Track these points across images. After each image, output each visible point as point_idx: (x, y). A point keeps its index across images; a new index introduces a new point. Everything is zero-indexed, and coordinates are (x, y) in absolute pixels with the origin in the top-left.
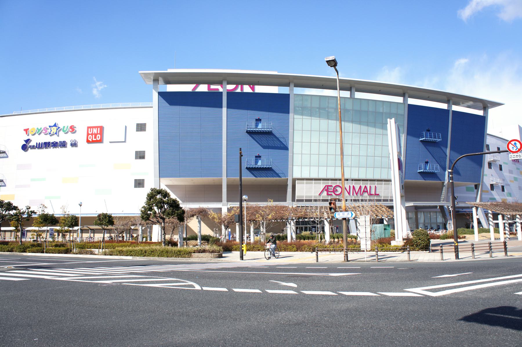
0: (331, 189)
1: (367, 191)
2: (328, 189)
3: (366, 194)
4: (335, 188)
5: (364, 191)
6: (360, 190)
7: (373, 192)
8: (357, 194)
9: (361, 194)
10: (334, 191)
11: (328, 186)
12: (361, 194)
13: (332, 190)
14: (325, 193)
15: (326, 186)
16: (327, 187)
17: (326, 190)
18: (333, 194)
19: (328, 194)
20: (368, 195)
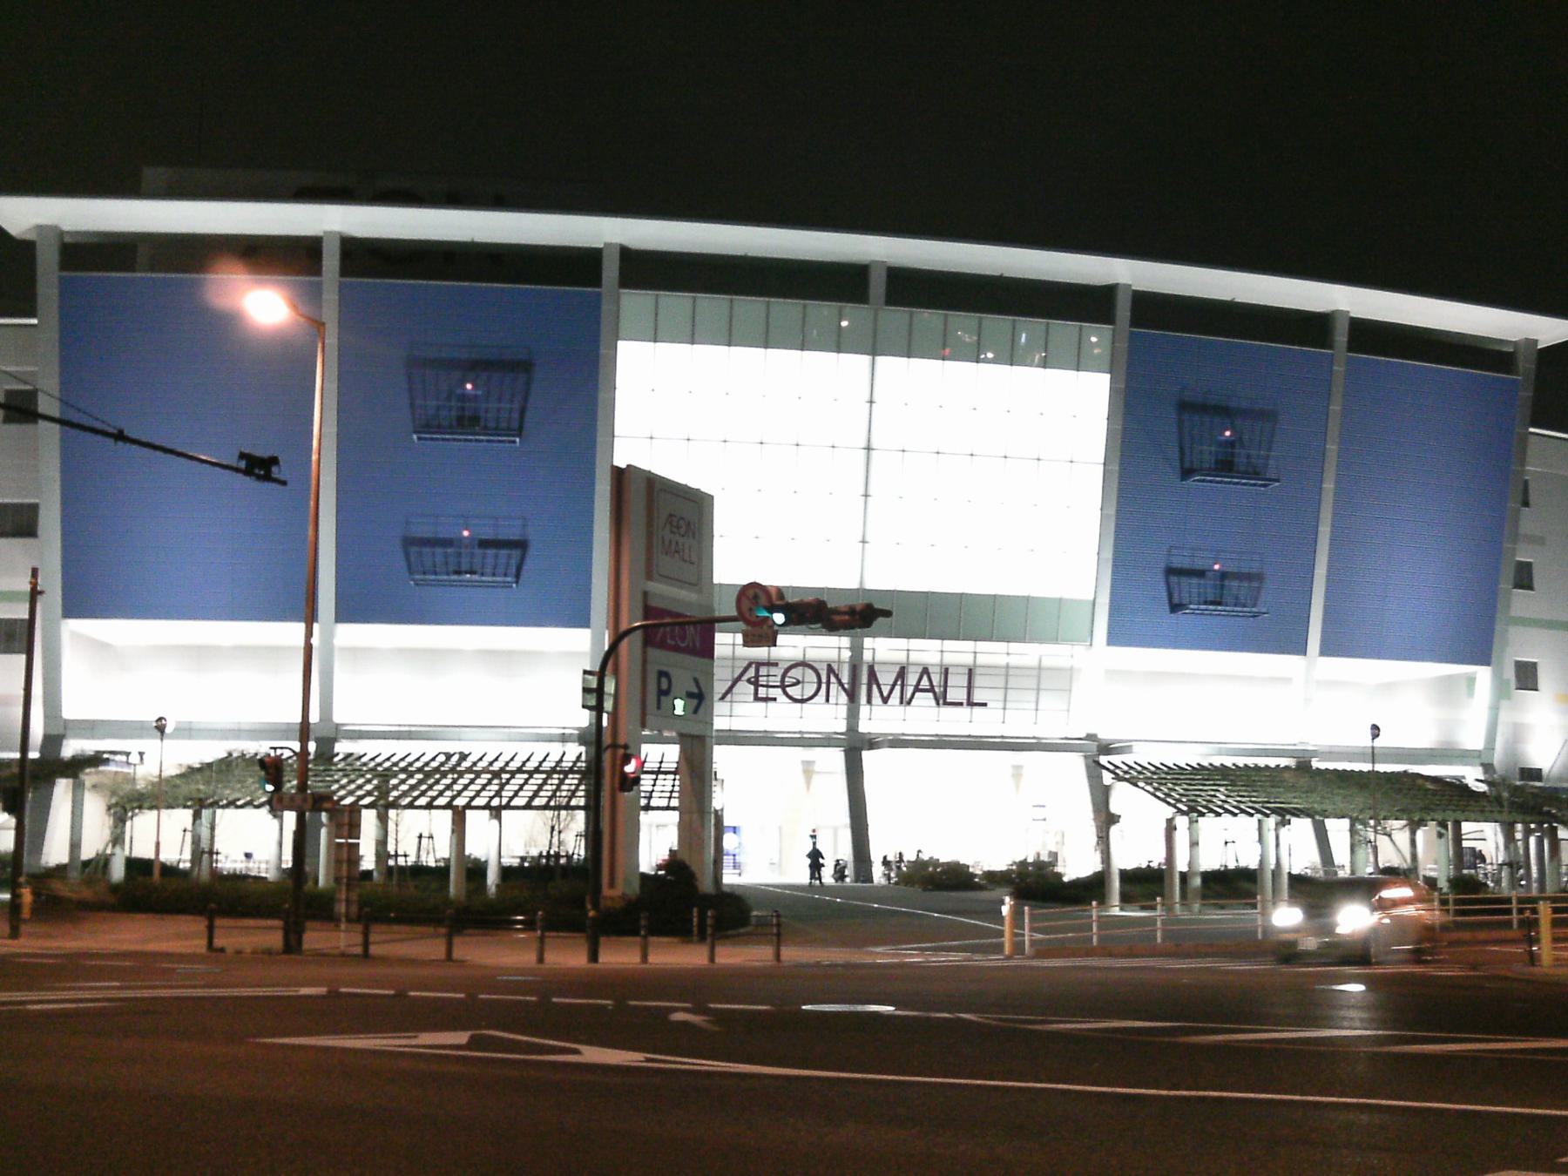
2: (757, 676)
4: (789, 674)
5: (917, 689)
6: (898, 688)
8: (885, 700)
10: (783, 687)
13: (778, 684)
15: (749, 665)
16: (757, 671)
17: (749, 681)
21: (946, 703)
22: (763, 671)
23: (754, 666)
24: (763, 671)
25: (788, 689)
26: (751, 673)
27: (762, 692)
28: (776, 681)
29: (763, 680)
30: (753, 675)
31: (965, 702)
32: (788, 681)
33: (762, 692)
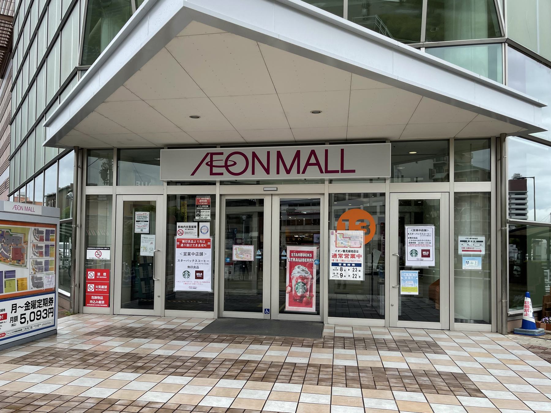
0: (219, 161)
1: (318, 164)
3: (313, 173)
5: (308, 164)
7: (334, 164)
8: (288, 172)
9: (301, 170)
10: (226, 166)
11: (212, 154)
12: (301, 170)
14: (205, 168)
15: (208, 154)
17: (207, 164)
18: (223, 170)
19: (212, 174)
20: (322, 172)
21: (327, 171)
22: (215, 157)
23: (209, 156)
24: (215, 157)
25: (230, 168)
26: (208, 159)
27: (215, 170)
28: (223, 163)
29: (214, 163)
30: (210, 161)
31: (340, 169)
32: (229, 163)
33: (215, 170)
